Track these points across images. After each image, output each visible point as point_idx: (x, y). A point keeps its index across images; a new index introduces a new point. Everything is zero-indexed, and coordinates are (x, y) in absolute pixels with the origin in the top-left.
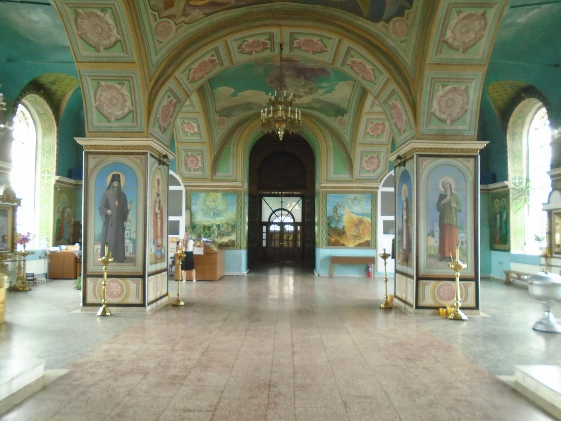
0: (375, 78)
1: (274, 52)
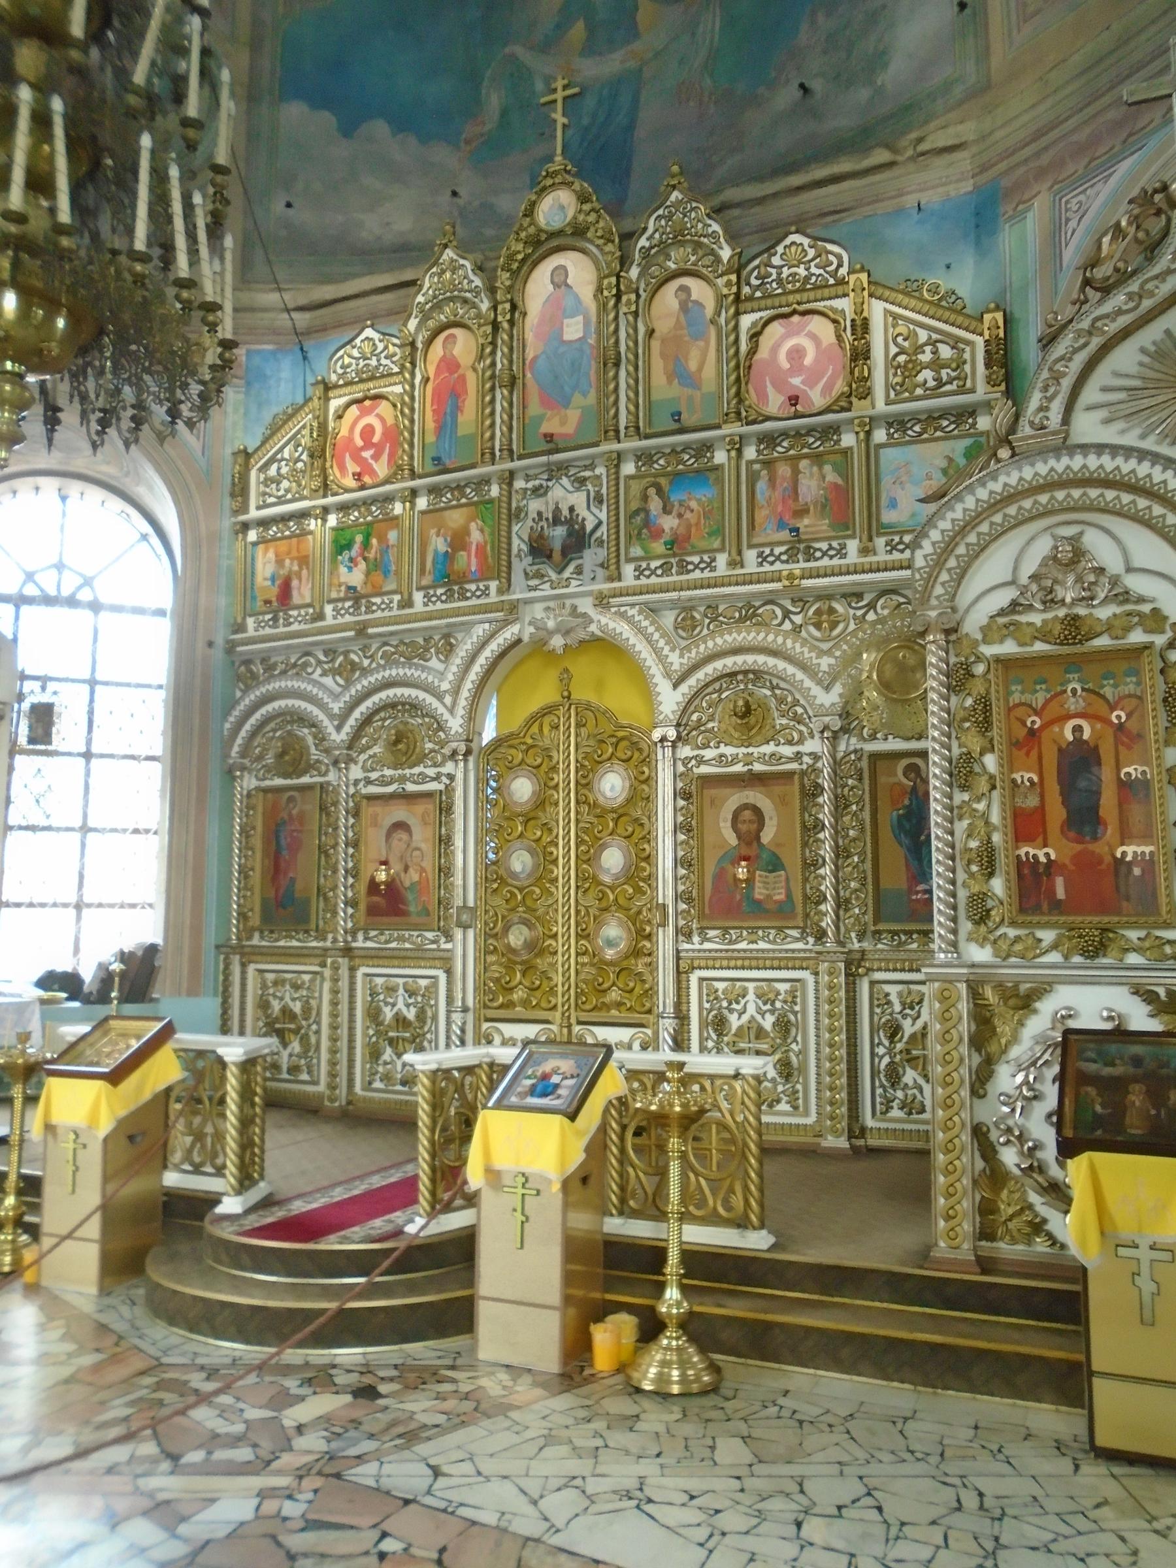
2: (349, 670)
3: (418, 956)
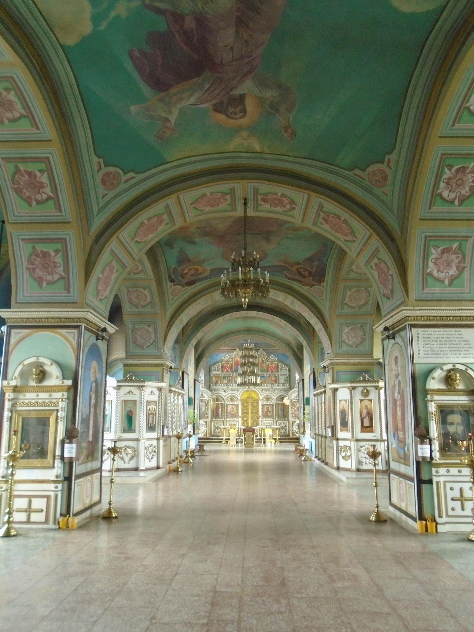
0: (137, 242)
1: (254, 188)
2: (225, 391)
3: (235, 421)
